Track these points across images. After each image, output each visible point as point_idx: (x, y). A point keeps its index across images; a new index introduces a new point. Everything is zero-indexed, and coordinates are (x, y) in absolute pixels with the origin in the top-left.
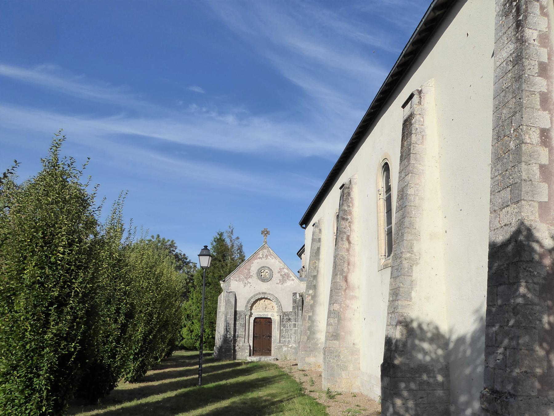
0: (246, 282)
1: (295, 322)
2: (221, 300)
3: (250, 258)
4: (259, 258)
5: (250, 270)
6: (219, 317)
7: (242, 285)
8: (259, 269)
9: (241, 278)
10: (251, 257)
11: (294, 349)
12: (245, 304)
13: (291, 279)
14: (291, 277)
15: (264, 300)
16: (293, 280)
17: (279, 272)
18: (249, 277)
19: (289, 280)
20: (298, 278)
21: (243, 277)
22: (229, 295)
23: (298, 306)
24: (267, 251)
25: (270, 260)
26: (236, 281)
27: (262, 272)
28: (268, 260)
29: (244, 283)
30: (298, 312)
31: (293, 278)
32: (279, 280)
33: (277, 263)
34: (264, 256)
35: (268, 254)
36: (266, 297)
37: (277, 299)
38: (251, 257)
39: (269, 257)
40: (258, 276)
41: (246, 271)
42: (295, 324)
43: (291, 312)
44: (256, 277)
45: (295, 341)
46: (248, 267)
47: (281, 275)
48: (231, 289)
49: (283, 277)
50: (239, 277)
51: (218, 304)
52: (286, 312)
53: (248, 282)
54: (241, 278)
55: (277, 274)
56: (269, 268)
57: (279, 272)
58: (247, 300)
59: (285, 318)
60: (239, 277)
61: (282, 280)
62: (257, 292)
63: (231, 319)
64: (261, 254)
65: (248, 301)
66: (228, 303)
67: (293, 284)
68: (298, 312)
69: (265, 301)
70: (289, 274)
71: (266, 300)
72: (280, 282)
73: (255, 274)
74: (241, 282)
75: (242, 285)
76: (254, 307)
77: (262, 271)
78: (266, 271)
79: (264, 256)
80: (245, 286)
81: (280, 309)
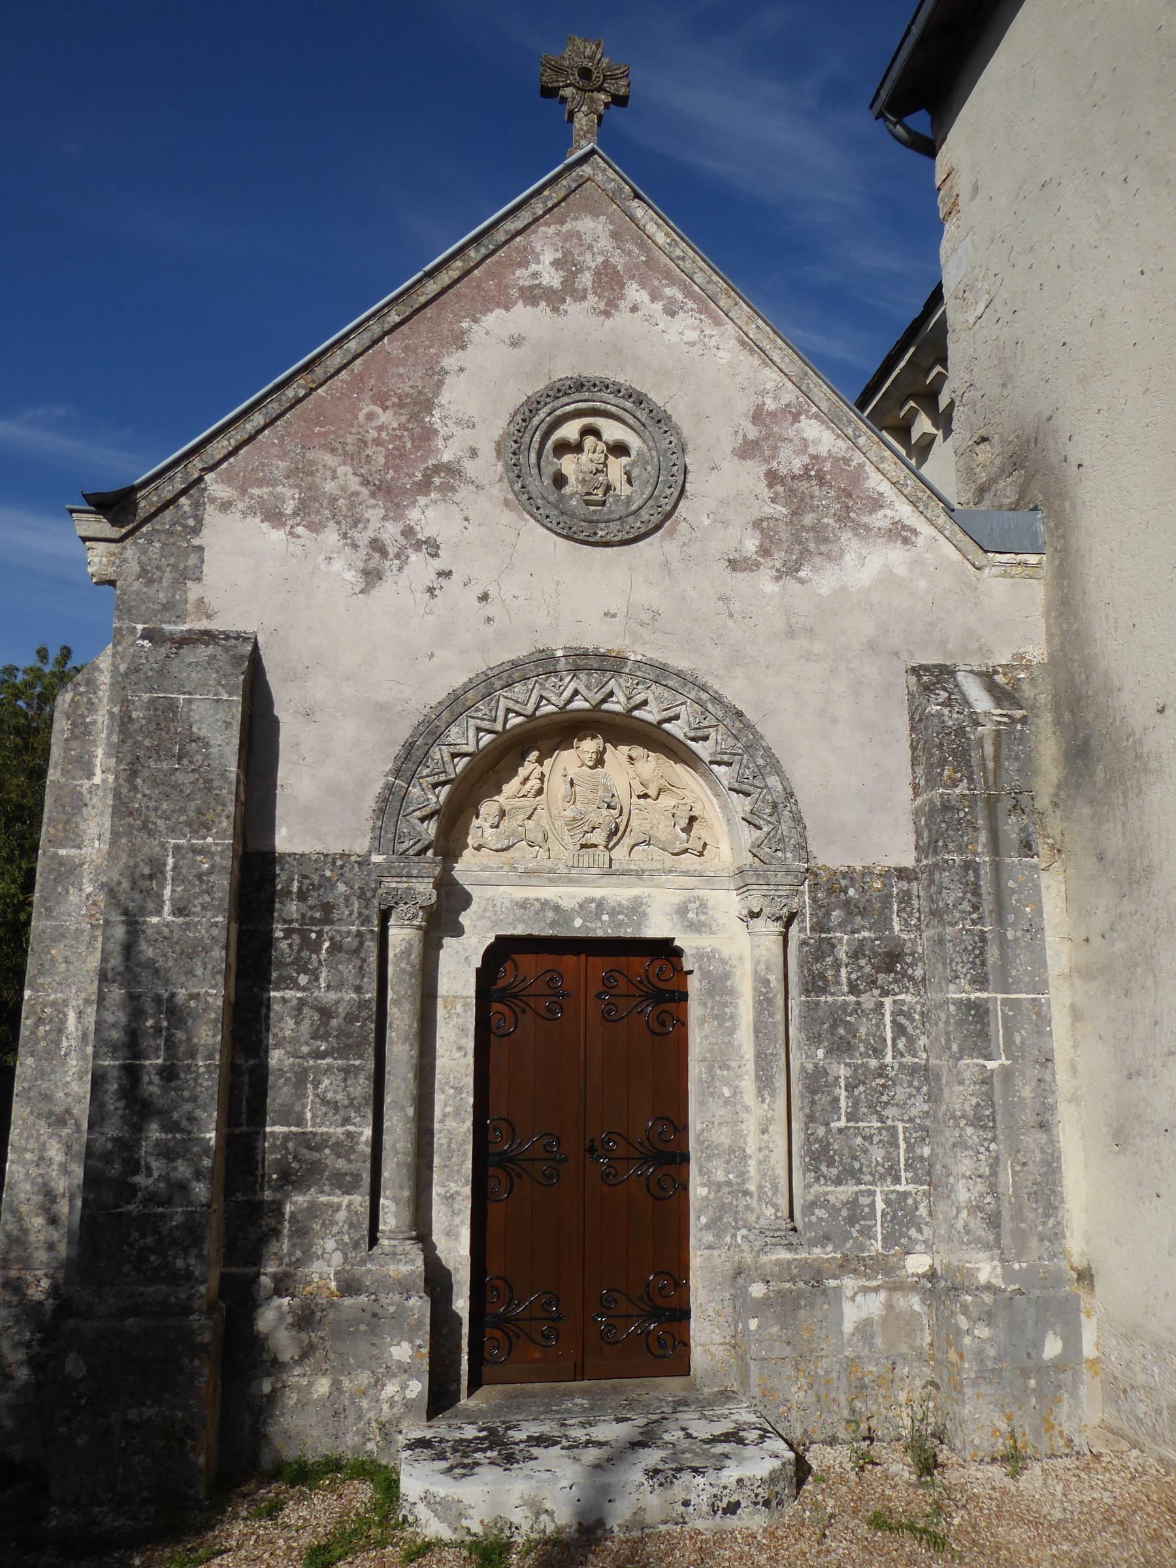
0: (391, 533)
1: (980, 982)
2: (82, 731)
3: (432, 287)
4: (533, 295)
5: (428, 406)
6: (60, 935)
7: (338, 565)
8: (532, 406)
9: (330, 487)
10: (445, 278)
11: (988, 1317)
12: (377, 788)
13: (879, 520)
14: (876, 503)
15: (590, 746)
16: (901, 534)
17: (747, 450)
18: (424, 486)
19: (863, 531)
20: (949, 509)
21: (354, 484)
22: (175, 666)
23: (992, 803)
24: (616, 236)
25: (649, 318)
26: (274, 517)
27: (563, 448)
28: (622, 318)
29: (363, 538)
30: (997, 867)
31: (904, 511)
32: (757, 524)
33: (724, 356)
34: (586, 279)
35: (619, 261)
36: (616, 706)
37: (749, 727)
38: (445, 278)
39: (635, 293)
40: (516, 472)
41: (385, 417)
42: (978, 1012)
43: (902, 873)
44: (500, 491)
45: (994, 1221)
46: (406, 380)
47: (772, 477)
48: (213, 602)
49: (798, 505)
50: (301, 472)
51: (53, 775)
52: (849, 874)
53: (408, 532)
54: (330, 487)
55: (730, 465)
56: (640, 399)
57: (747, 450)
58: (403, 734)
59: (844, 942)
60: (301, 472)
61: (784, 534)
62: (520, 649)
63: (190, 952)
64: (548, 257)
65: (409, 747)
66: (157, 752)
67: (902, 571)
68: (997, 867)
69: (600, 762)
70: (858, 476)
71: (617, 756)
72: (765, 552)
73: (487, 450)
74: (331, 536)
75: (338, 565)
76: (542, 464)
77: (570, 431)
78: (612, 431)
79: (586, 279)
80: (371, 577)
81: (777, 842)
